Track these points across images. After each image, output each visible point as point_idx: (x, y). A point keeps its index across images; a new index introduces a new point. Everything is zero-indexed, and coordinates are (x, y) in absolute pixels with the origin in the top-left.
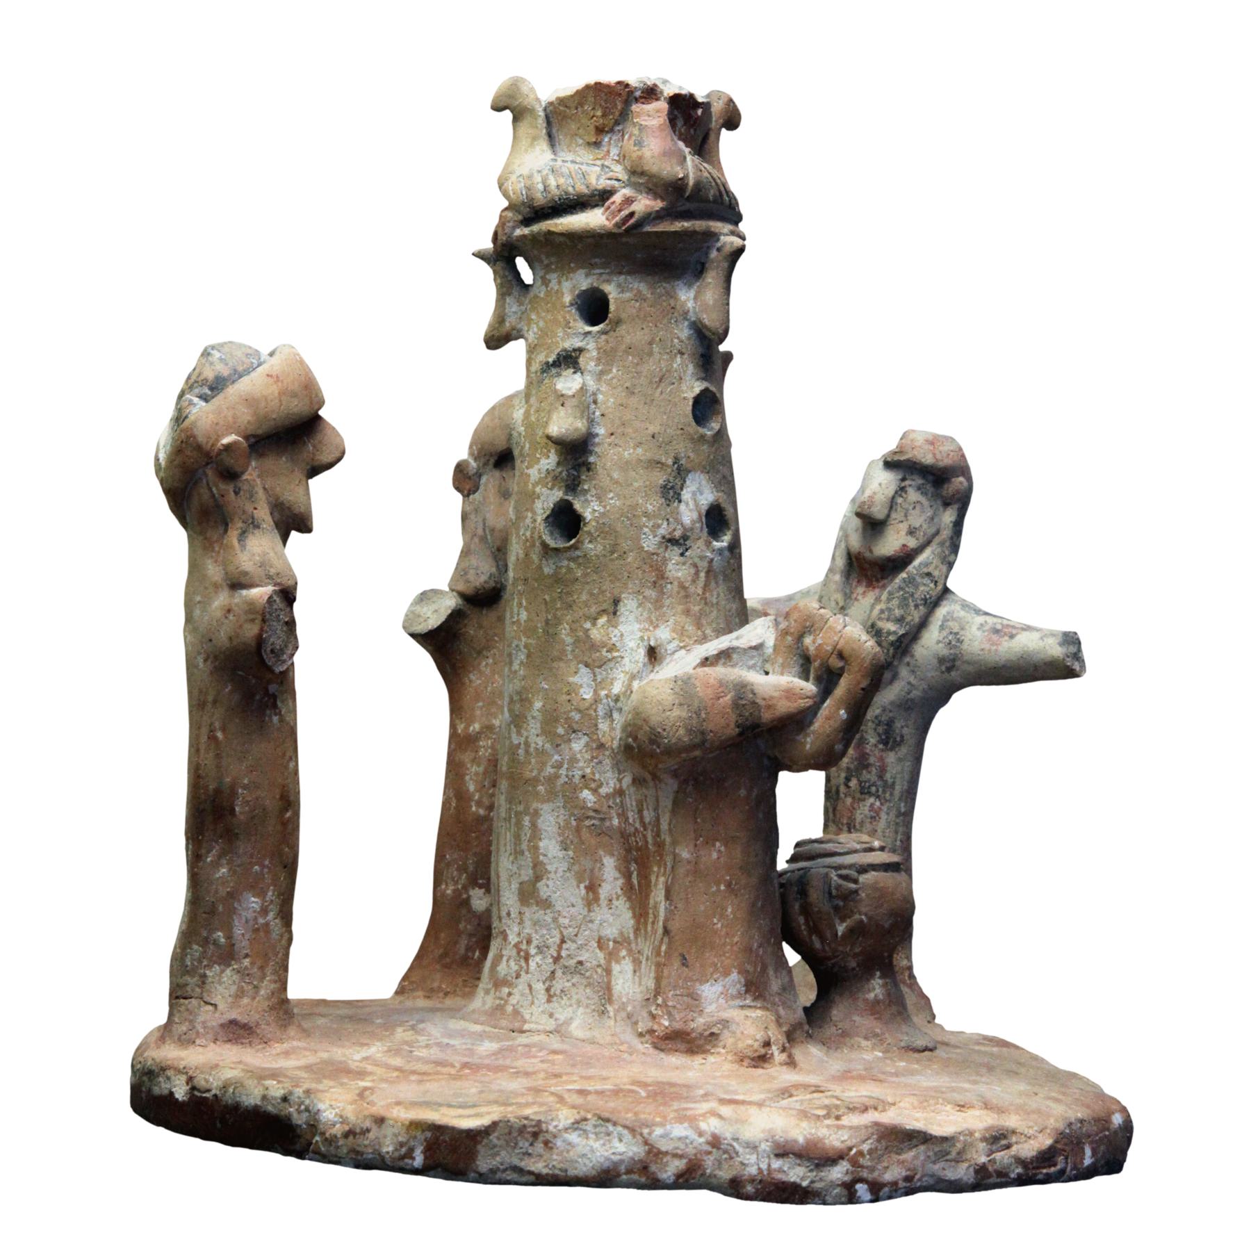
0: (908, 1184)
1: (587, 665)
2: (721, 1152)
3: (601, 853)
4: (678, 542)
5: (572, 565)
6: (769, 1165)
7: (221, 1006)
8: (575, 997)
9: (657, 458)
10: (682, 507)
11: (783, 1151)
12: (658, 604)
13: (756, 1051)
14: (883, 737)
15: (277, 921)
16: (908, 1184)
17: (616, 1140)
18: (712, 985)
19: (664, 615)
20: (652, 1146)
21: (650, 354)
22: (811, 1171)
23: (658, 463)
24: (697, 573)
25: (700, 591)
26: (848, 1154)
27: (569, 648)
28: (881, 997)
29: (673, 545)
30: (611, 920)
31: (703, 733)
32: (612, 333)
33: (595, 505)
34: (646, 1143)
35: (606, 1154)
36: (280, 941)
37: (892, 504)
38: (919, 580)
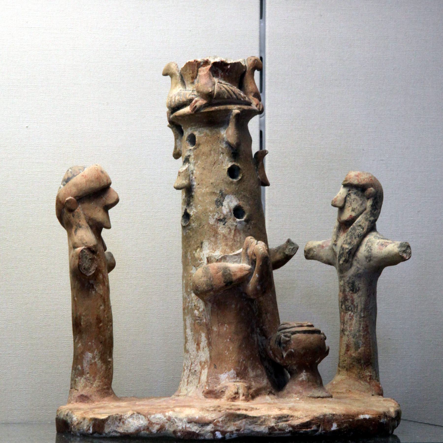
0: (237, 432)
1: (194, 266)
2: (170, 422)
3: (201, 332)
4: (222, 220)
5: (189, 232)
6: (186, 426)
7: (80, 390)
8: (194, 383)
9: (213, 191)
10: (223, 208)
11: (190, 421)
12: (216, 243)
13: (232, 396)
14: (351, 288)
15: (99, 361)
16: (237, 432)
17: (141, 420)
18: (224, 374)
19: (218, 246)
20: (150, 421)
21: (211, 154)
22: (200, 427)
23: (214, 193)
24: (230, 230)
25: (232, 237)
26: (213, 422)
27: (190, 261)
28: (305, 379)
29: (220, 221)
30: (203, 355)
31: (212, 286)
32: (197, 149)
33: (194, 210)
34: (149, 420)
35: (138, 424)
36: (101, 368)
37: (345, 200)
38: (356, 228)
